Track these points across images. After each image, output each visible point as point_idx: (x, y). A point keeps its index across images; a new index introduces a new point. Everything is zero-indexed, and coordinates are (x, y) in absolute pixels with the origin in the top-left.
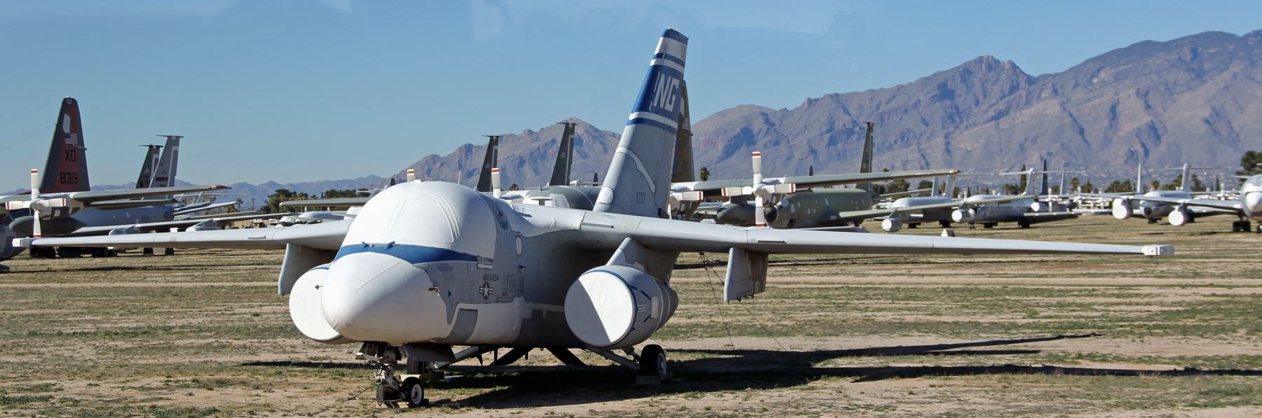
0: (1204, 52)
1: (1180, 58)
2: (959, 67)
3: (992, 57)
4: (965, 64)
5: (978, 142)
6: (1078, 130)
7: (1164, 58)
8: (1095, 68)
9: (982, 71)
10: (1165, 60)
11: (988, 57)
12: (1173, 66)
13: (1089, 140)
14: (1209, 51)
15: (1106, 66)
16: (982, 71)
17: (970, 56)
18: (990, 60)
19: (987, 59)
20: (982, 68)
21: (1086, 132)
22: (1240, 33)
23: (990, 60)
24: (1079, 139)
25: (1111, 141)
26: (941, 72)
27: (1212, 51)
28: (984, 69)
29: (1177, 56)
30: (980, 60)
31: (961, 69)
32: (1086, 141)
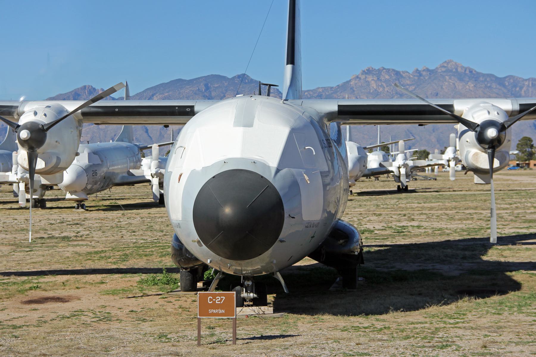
0: (212, 86)
1: (199, 89)
2: (72, 91)
3: (92, 86)
4: (75, 90)
5: (87, 136)
6: (145, 130)
7: (191, 89)
8: (151, 94)
9: (86, 94)
10: (191, 90)
11: (89, 86)
12: (195, 94)
13: (151, 136)
14: (214, 86)
15: (157, 93)
16: (86, 94)
17: (80, 85)
18: (90, 88)
19: (88, 88)
20: (85, 93)
21: (149, 131)
22: (230, 76)
23: (90, 88)
24: (145, 135)
25: (164, 137)
26: (61, 94)
27: (216, 86)
28: (87, 93)
29: (198, 88)
30: (85, 87)
31: (73, 93)
32: (150, 136)
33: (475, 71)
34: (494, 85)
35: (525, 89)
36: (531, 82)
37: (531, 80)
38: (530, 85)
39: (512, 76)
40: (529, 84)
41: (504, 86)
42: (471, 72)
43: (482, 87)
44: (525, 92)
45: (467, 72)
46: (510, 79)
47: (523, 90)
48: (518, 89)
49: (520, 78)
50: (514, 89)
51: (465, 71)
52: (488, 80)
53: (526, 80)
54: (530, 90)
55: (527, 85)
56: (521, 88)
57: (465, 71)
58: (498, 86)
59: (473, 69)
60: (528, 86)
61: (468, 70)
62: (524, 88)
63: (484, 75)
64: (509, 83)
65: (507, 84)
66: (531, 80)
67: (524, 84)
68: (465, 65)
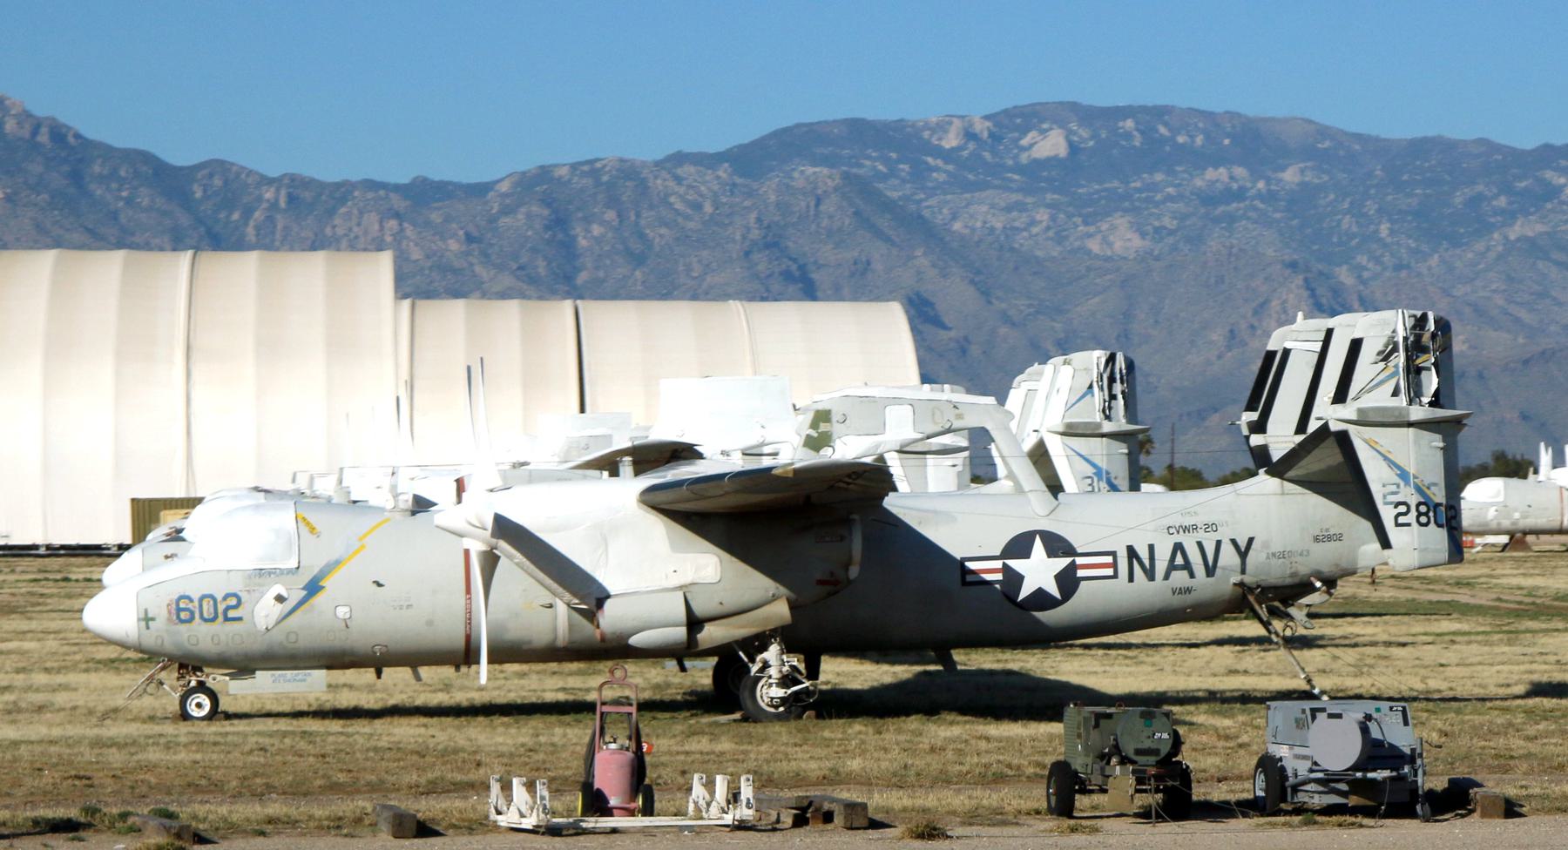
33: (78, 136)
34: (144, 197)
35: (258, 215)
36: (283, 192)
37: (286, 181)
38: (282, 204)
39: (221, 163)
40: (277, 200)
41: (186, 202)
42: (59, 133)
43: (36, 205)
44: (258, 228)
45: (43, 137)
46: (211, 176)
47: (252, 223)
48: (236, 216)
49: (250, 173)
50: (222, 215)
51: (35, 131)
52: (123, 173)
53: (270, 181)
54: (281, 221)
55: (268, 201)
56: (248, 213)
57: (35, 131)
58: (160, 202)
59: (69, 128)
60: (274, 205)
61: (44, 130)
62: (257, 214)
63: (107, 151)
64: (205, 191)
65: (199, 195)
66: (286, 181)
67: (260, 199)
68: (40, 111)
